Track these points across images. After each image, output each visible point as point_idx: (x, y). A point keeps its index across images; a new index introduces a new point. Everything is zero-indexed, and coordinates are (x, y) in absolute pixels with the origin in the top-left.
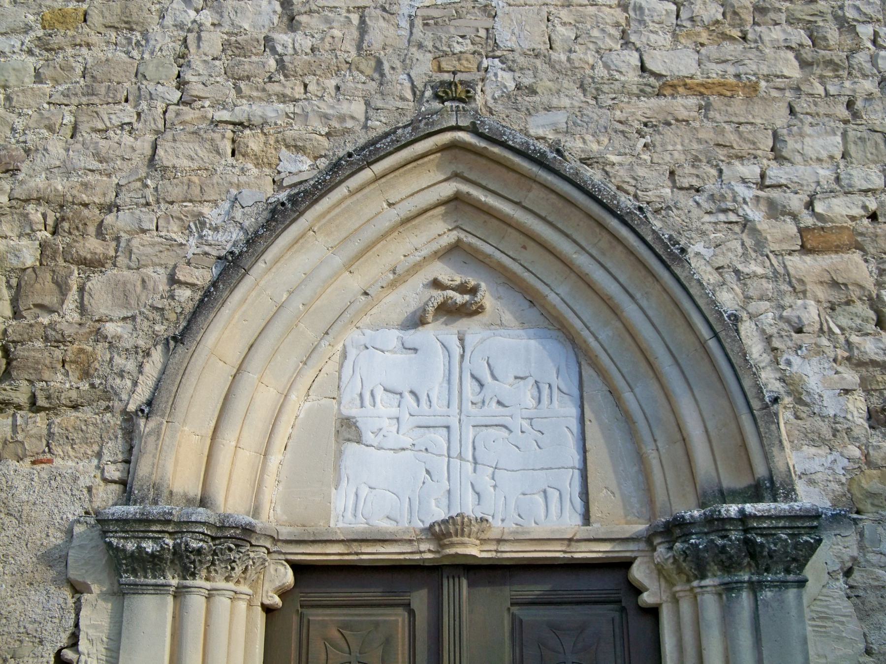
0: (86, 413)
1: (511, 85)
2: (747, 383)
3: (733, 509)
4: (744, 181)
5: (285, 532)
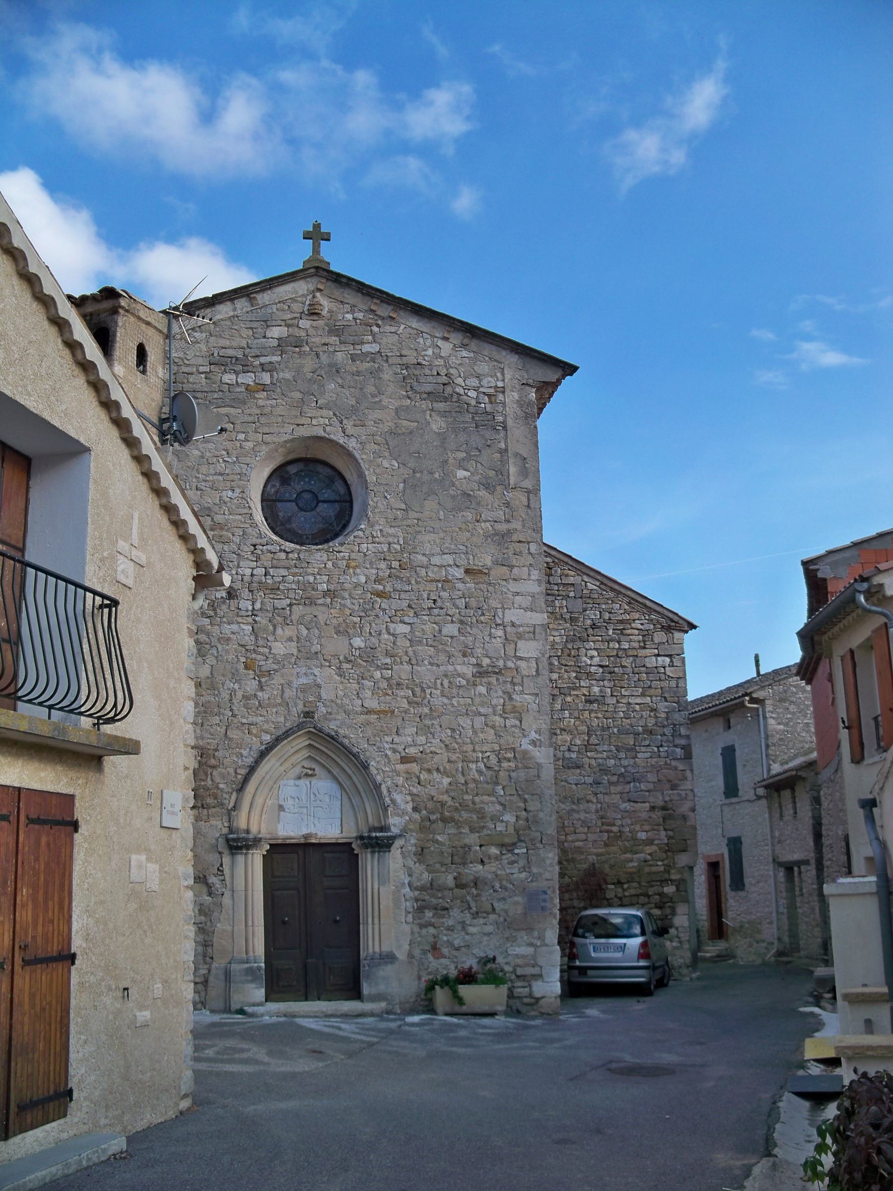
0: (217, 809)
1: (325, 712)
2: (382, 802)
3: (374, 834)
4: (387, 742)
5: (268, 836)
